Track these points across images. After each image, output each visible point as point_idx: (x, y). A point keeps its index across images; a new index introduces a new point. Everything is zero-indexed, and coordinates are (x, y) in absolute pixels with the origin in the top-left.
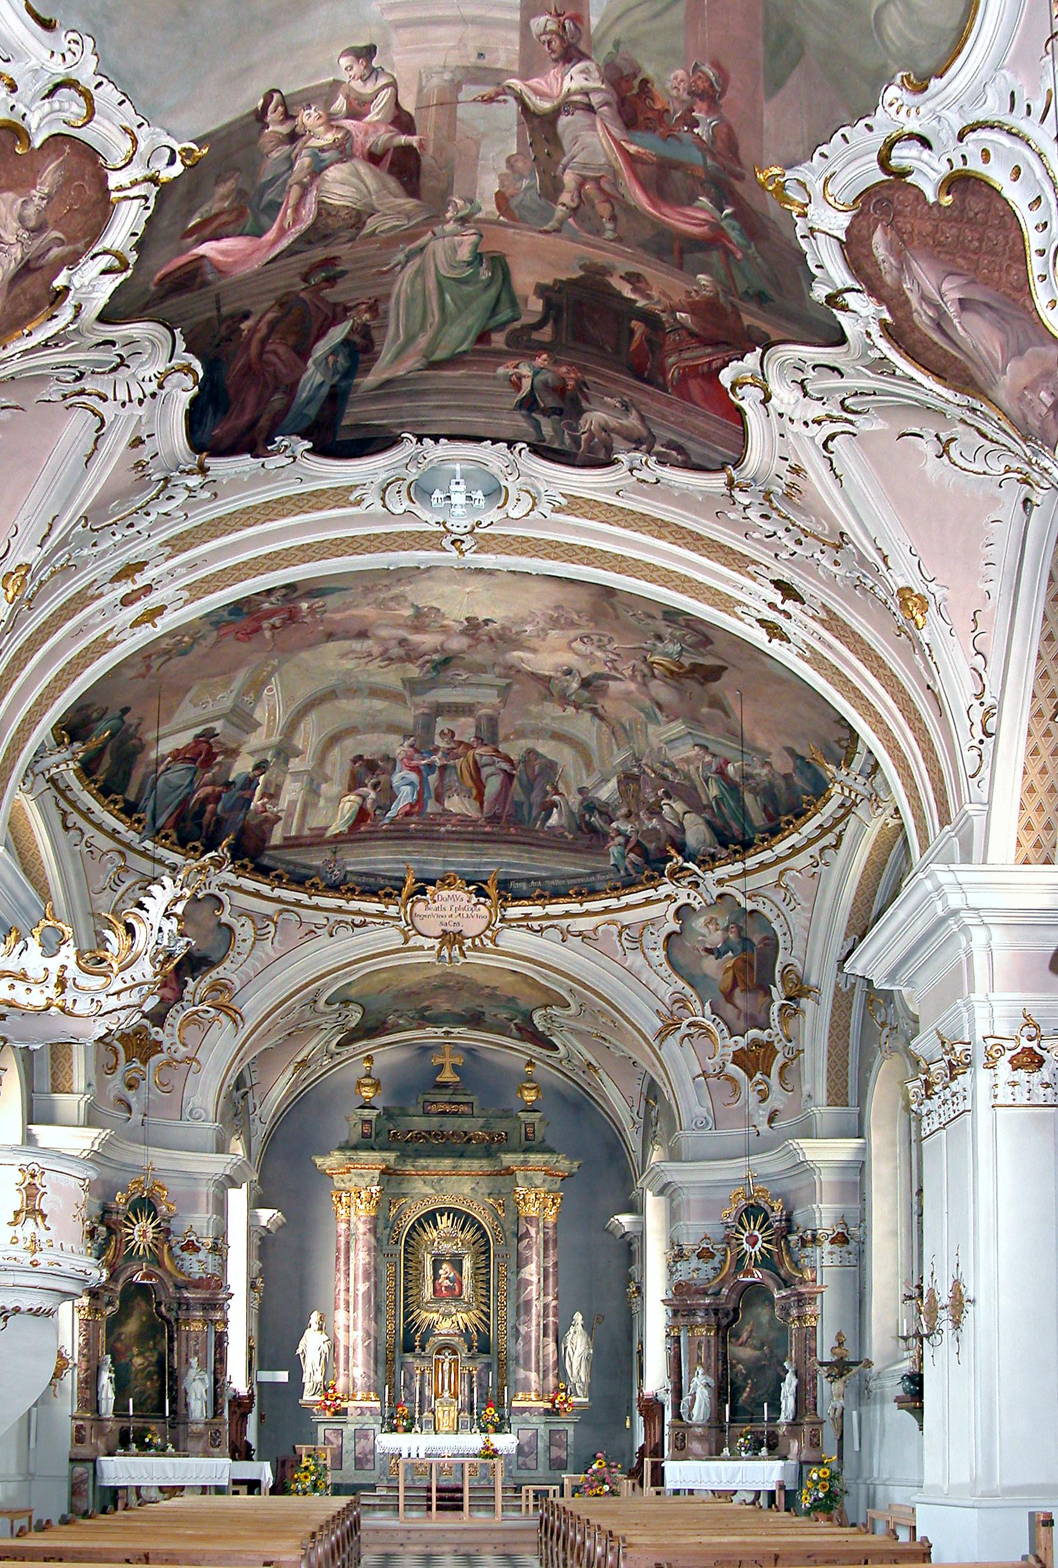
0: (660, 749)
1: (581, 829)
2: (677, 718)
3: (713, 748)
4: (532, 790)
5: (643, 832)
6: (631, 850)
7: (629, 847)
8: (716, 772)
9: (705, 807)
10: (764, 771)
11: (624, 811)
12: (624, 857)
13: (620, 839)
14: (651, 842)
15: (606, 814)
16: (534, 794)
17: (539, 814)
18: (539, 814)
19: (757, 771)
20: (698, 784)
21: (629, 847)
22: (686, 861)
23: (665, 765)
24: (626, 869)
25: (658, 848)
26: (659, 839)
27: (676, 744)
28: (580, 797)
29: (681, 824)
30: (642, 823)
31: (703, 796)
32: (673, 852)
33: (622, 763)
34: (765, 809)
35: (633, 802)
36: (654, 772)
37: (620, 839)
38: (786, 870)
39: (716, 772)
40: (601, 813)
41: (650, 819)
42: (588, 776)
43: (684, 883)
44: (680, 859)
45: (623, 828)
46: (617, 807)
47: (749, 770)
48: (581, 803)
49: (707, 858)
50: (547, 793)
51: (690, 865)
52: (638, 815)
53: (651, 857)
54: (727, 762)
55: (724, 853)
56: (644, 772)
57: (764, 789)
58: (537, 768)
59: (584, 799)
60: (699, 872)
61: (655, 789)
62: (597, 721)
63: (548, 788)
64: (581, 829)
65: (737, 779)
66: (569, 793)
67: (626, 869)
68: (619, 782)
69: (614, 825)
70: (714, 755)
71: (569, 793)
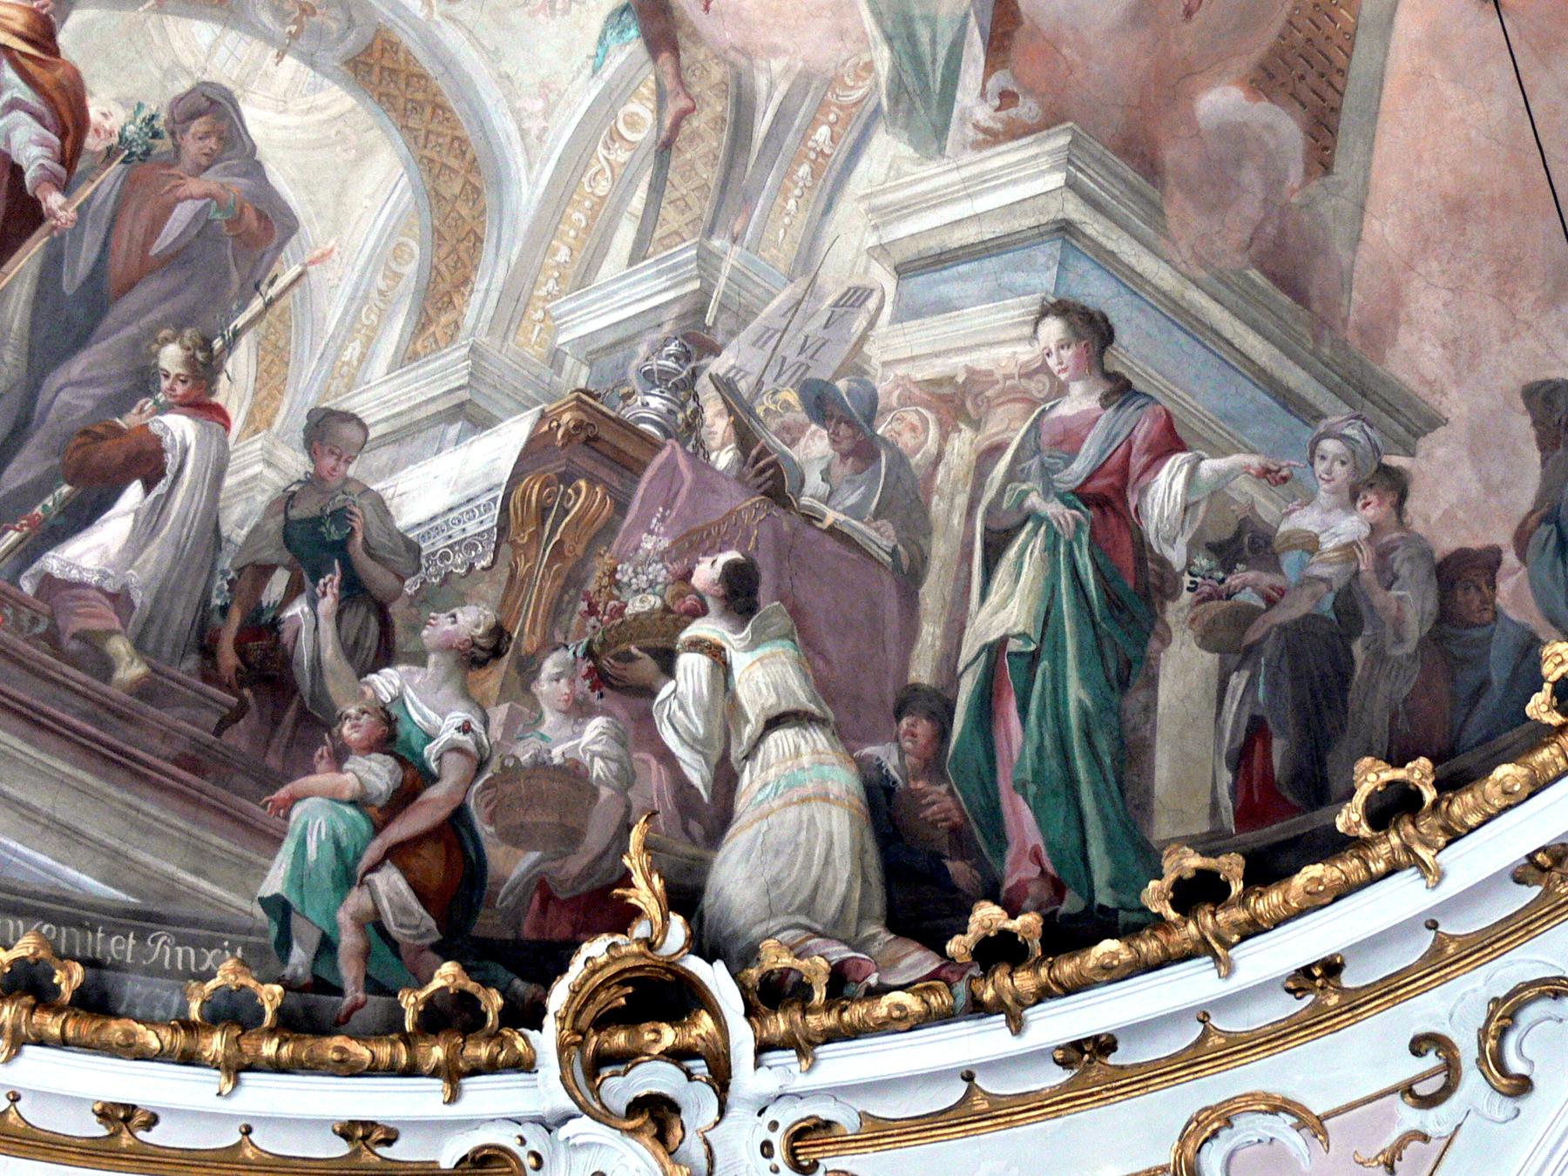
0: (855, 297)
1: (207, 649)
2: (1051, 119)
3: (1128, 354)
4: (81, 339)
5: (511, 773)
6: (397, 854)
7: (401, 829)
8: (1084, 496)
9: (908, 700)
10: (1349, 526)
11: (471, 620)
12: (348, 876)
13: (377, 774)
14: (516, 837)
15: (382, 611)
16: (77, 367)
17: (41, 488)
18: (41, 488)
19: (1306, 520)
20: (941, 550)
21: (401, 829)
22: (705, 945)
23: (820, 403)
24: (327, 946)
25: (542, 888)
26: (571, 837)
27: (947, 285)
28: (296, 463)
29: (726, 779)
30: (527, 718)
31: (930, 633)
32: (645, 893)
33: (596, 351)
34: (1241, 759)
35: (543, 588)
36: (744, 436)
37: (377, 774)
38: (1222, 1117)
39: (1084, 496)
40: (353, 588)
41: (579, 710)
42: (407, 358)
43: (621, 1088)
44: (678, 931)
45: (420, 712)
46: (446, 594)
47: (1266, 506)
48: (289, 499)
49: (816, 969)
50: (144, 379)
51: (716, 978)
52: (528, 669)
53: (487, 924)
54: (1169, 441)
55: (917, 961)
56: (693, 424)
57: (1298, 635)
58: (182, 214)
59: (313, 482)
60: (742, 1037)
61: (692, 544)
62: (630, 47)
63: (171, 357)
64: (207, 649)
65: (1177, 556)
66: (255, 423)
67: (327, 946)
68: (534, 452)
69: (386, 682)
70: (1120, 390)
71: (255, 423)
